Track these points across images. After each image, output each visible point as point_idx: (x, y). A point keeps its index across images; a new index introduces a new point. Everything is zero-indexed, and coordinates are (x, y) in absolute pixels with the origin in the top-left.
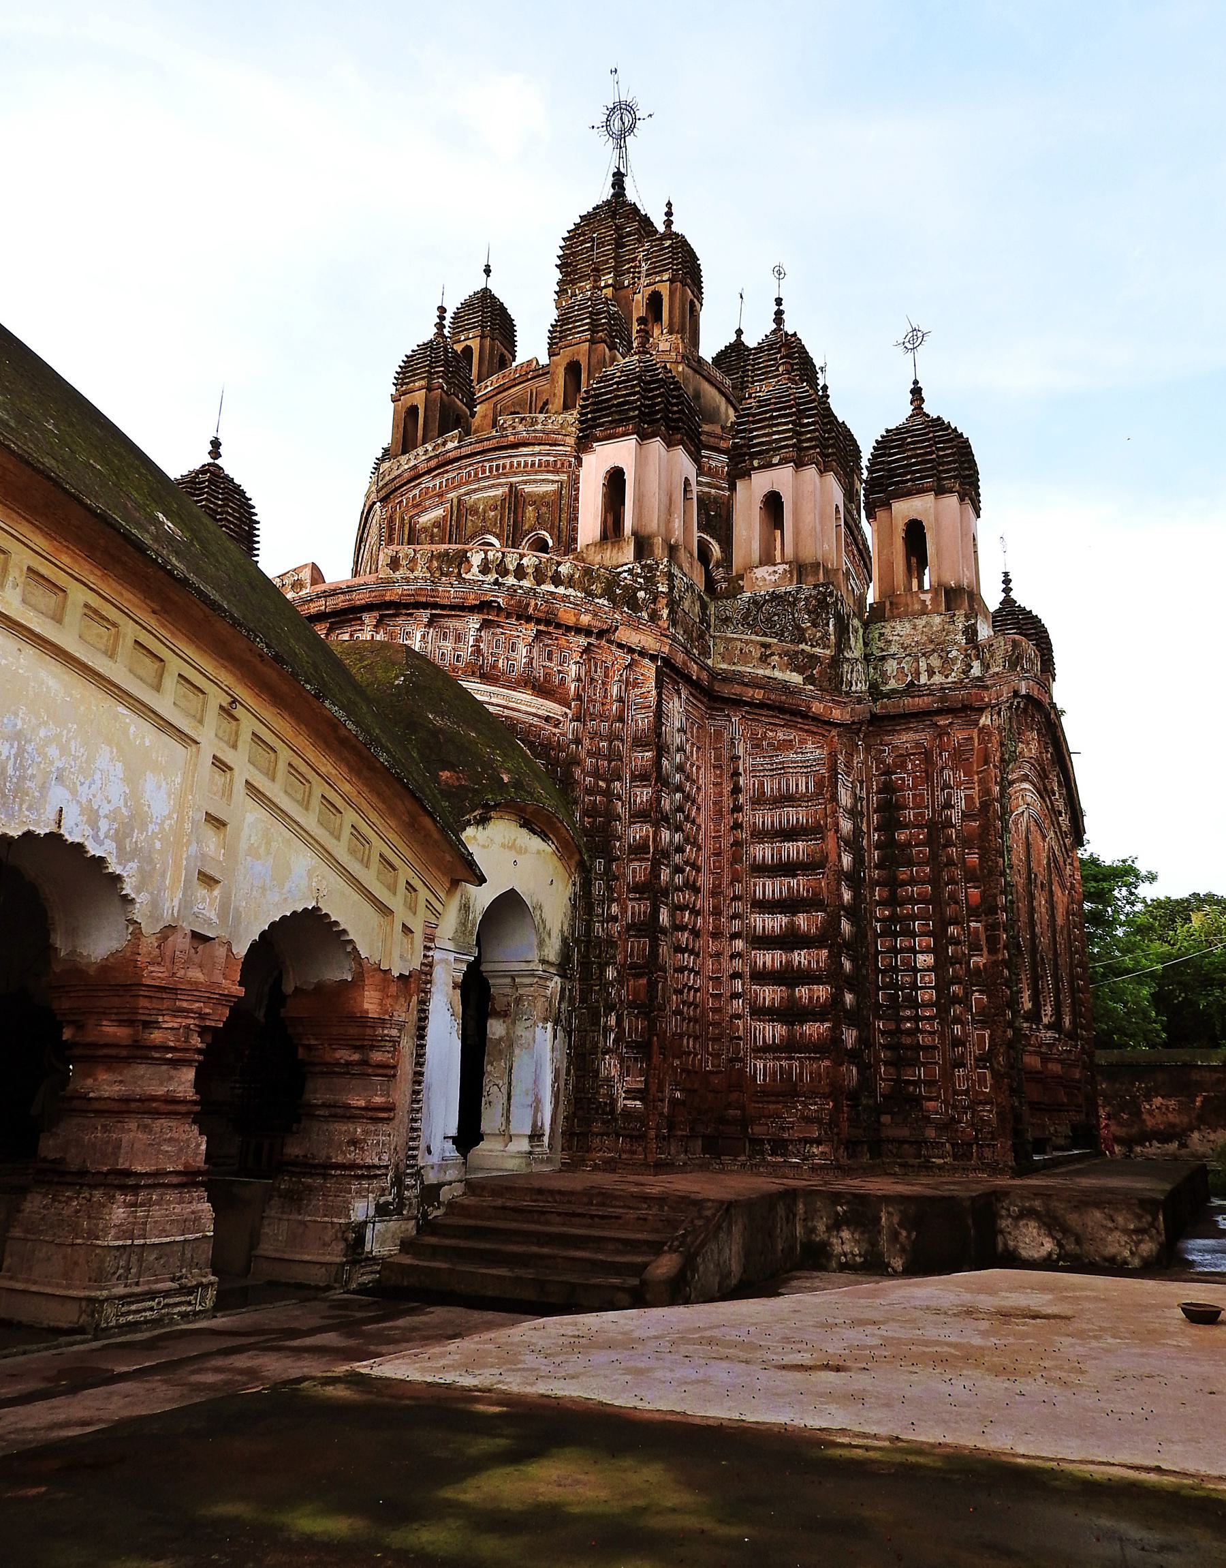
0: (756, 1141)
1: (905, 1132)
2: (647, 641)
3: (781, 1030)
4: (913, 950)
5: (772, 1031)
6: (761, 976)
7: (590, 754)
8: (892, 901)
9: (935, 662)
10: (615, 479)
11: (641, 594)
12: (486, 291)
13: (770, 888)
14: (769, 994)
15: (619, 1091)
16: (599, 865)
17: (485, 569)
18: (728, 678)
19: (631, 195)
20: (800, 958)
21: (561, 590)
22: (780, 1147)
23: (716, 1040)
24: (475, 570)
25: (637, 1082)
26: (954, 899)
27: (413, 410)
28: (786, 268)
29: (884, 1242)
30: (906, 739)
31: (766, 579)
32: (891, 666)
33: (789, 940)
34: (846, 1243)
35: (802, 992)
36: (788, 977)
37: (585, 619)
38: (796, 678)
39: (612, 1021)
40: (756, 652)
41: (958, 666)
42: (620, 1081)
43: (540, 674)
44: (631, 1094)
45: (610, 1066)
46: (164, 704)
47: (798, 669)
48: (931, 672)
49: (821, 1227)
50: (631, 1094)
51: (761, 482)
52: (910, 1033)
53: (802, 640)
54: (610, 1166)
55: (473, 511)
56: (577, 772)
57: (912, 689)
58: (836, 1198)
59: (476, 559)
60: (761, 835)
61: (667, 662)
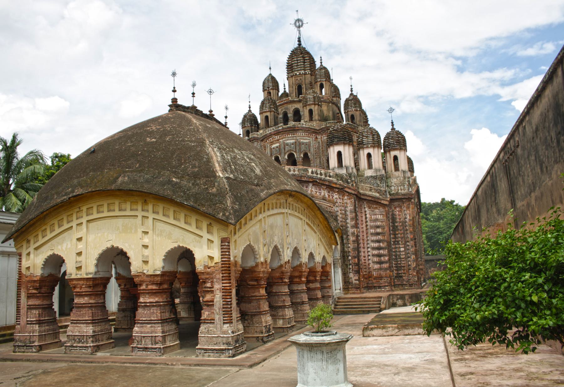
0: (374, 287)
1: (400, 283)
2: (353, 192)
3: (378, 266)
4: (400, 248)
5: (377, 266)
6: (373, 255)
7: (341, 214)
8: (395, 238)
9: (402, 188)
10: (339, 154)
11: (349, 180)
12: (270, 74)
13: (374, 238)
14: (376, 259)
15: (353, 279)
16: (345, 236)
17: (312, 173)
18: (364, 195)
19: (303, 45)
20: (382, 252)
21: (331, 179)
22: (380, 287)
23: (365, 268)
24: (310, 173)
25: (357, 278)
26: (408, 237)
27: (267, 117)
28: (352, 77)
29: (406, 301)
30: (396, 204)
31: (369, 173)
32: (393, 188)
33: (379, 248)
34: (400, 302)
35: (382, 258)
36: (379, 256)
37: (338, 186)
38: (378, 195)
39: (351, 267)
40: (369, 189)
41: (407, 189)
42: (353, 278)
43: (327, 196)
44: (356, 280)
45: (351, 275)
46: (315, 228)
47: (378, 193)
48: (401, 190)
49: (395, 300)
50: (356, 280)
51: (366, 151)
52: (400, 264)
53: (378, 186)
54: (354, 293)
55: (287, 145)
56: (339, 218)
57: (397, 194)
58: (397, 295)
59: (310, 170)
60: (372, 227)
61: (356, 195)
